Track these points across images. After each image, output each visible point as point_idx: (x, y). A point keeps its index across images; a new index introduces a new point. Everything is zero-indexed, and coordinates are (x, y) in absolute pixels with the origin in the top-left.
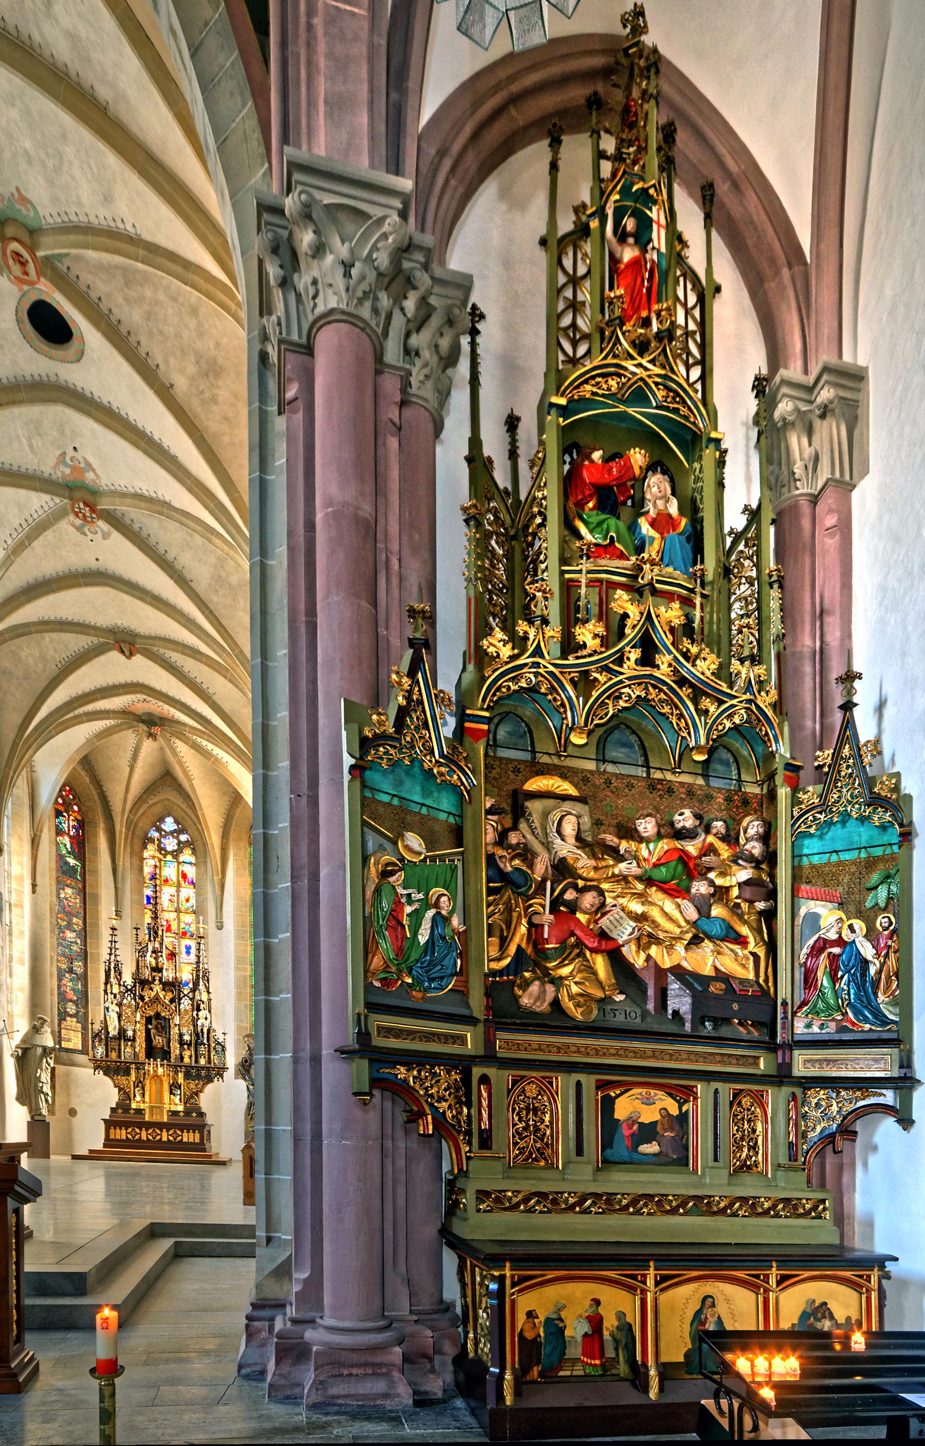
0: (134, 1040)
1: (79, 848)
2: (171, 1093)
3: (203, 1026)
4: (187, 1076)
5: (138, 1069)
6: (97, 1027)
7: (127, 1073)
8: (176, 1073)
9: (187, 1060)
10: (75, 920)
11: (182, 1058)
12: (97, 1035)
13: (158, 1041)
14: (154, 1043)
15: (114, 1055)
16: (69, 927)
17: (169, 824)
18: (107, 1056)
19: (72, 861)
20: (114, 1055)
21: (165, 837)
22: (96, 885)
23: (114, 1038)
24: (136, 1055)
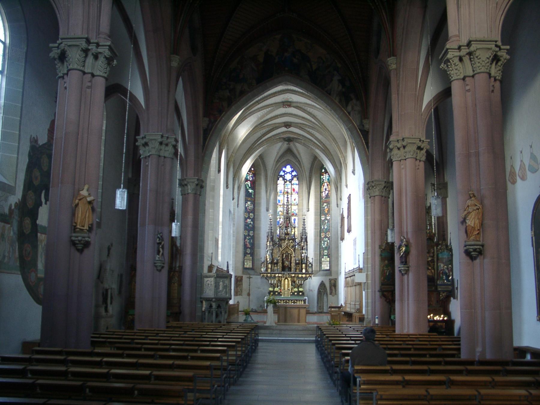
0: (277, 263)
1: (253, 185)
3: (304, 256)
10: (251, 214)
12: (263, 262)
13: (287, 263)
17: (288, 169)
19: (250, 191)
21: (286, 174)
22: (260, 198)
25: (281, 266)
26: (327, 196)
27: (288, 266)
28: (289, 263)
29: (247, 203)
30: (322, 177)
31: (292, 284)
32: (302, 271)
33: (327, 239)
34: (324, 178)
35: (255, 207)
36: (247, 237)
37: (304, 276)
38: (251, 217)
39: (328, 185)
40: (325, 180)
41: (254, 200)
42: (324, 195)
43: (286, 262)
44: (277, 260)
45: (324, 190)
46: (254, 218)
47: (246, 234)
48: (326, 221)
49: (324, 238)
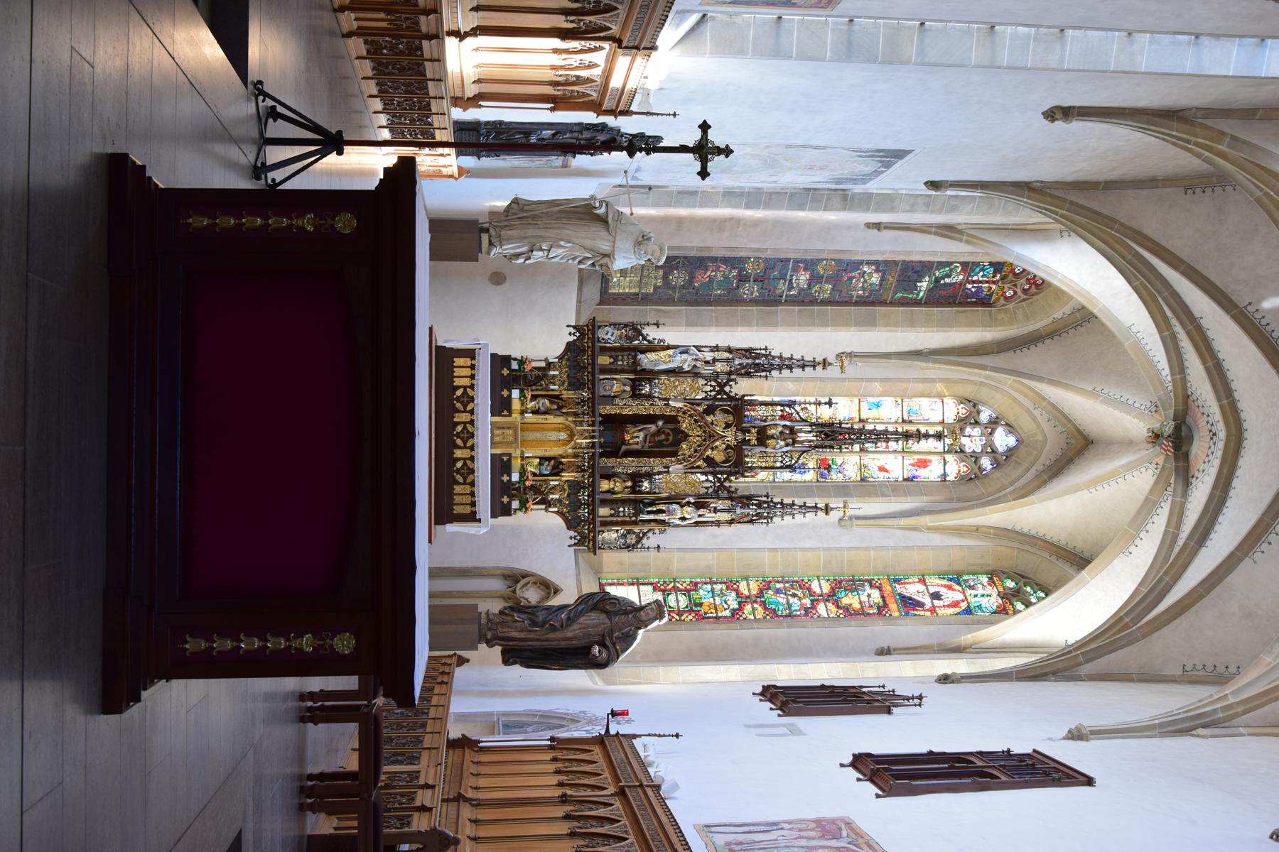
0: (636, 395)
2: (543, 459)
4: (575, 486)
5: (582, 402)
6: (652, 333)
7: (576, 385)
8: (580, 469)
9: (605, 485)
10: (828, 287)
11: (608, 477)
12: (640, 333)
13: (636, 437)
14: (631, 429)
15: (604, 360)
16: (815, 279)
18: (604, 350)
20: (604, 360)
23: (636, 363)
24: (610, 399)
25: (625, 412)
26: (909, 604)
27: (624, 442)
28: (639, 447)
29: (877, 271)
30: (985, 579)
31: (549, 459)
32: (604, 502)
33: (735, 605)
34: (980, 591)
35: (857, 303)
36: (734, 273)
37: (584, 512)
38: (817, 288)
39: (955, 604)
40: (973, 592)
41: (883, 303)
42: (913, 590)
43: (642, 435)
44: (649, 397)
45: (932, 590)
46: (813, 302)
47: (749, 268)
48: (807, 602)
49: (737, 591)
